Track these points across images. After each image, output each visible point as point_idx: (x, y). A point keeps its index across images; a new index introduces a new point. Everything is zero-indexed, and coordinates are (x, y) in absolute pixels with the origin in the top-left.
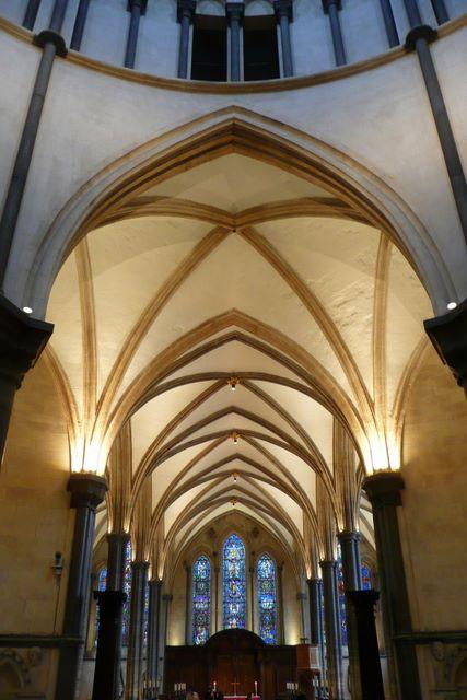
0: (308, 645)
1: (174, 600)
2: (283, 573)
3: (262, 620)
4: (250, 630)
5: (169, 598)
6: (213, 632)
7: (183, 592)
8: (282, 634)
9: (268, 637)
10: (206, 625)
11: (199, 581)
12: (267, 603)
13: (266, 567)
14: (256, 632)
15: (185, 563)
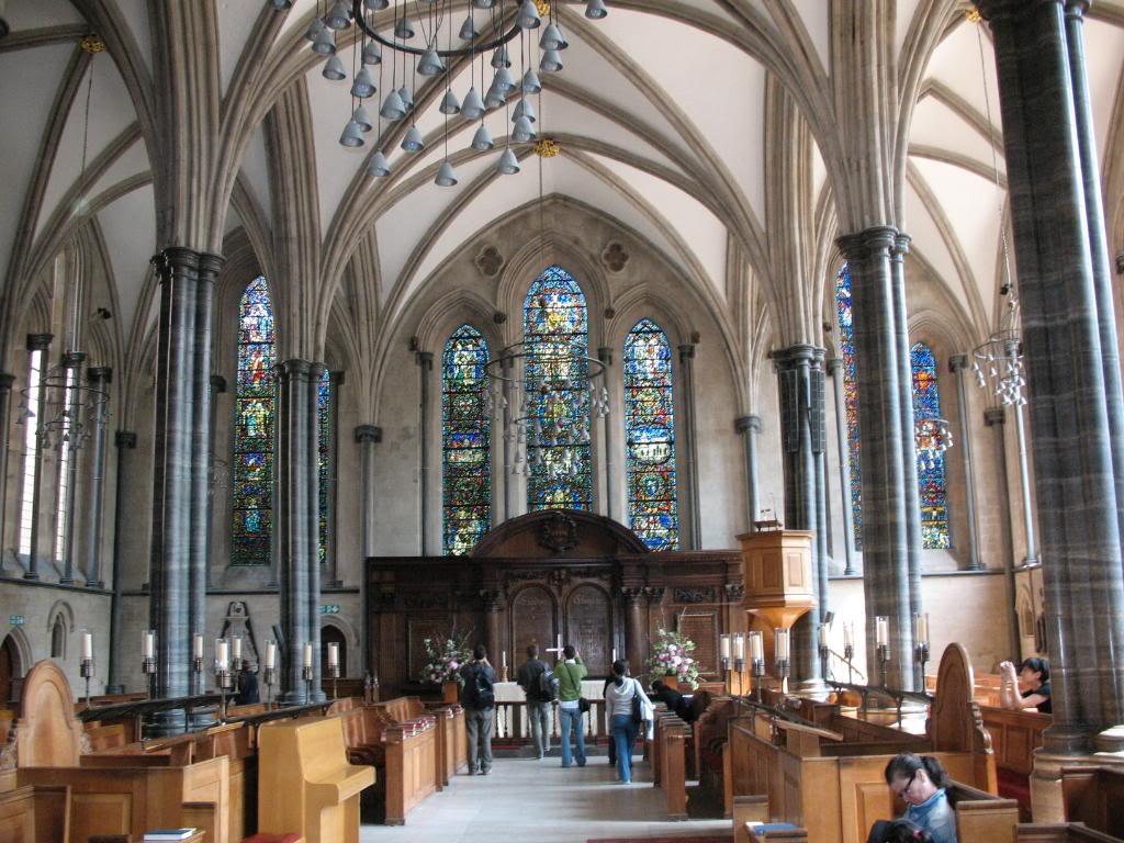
0: (778, 534)
1: (389, 438)
2: (698, 363)
3: (636, 487)
4: (603, 512)
5: (368, 436)
6: (500, 520)
7: (413, 420)
8: (689, 523)
9: (654, 531)
10: (480, 502)
11: (455, 390)
12: (652, 447)
13: (648, 354)
14: (625, 522)
15: (413, 344)
